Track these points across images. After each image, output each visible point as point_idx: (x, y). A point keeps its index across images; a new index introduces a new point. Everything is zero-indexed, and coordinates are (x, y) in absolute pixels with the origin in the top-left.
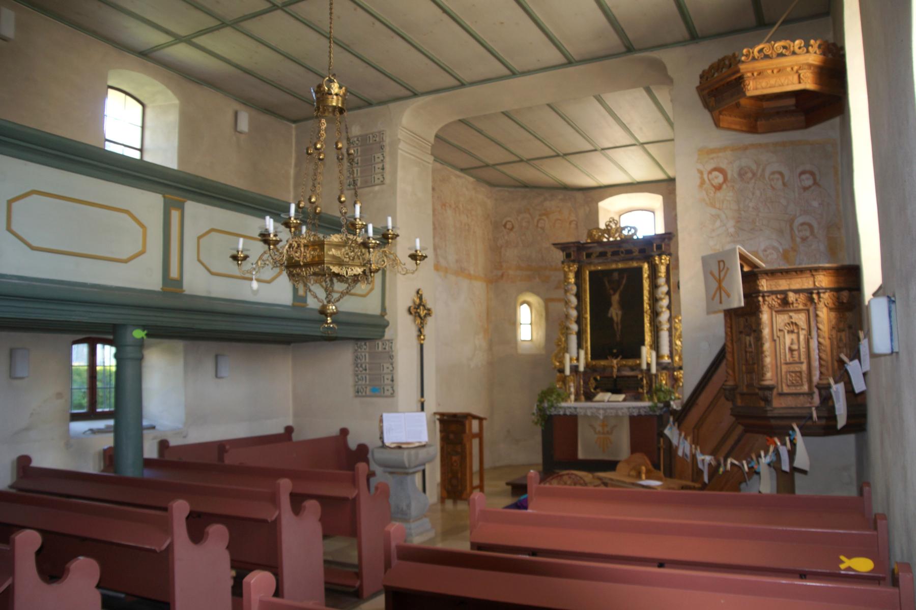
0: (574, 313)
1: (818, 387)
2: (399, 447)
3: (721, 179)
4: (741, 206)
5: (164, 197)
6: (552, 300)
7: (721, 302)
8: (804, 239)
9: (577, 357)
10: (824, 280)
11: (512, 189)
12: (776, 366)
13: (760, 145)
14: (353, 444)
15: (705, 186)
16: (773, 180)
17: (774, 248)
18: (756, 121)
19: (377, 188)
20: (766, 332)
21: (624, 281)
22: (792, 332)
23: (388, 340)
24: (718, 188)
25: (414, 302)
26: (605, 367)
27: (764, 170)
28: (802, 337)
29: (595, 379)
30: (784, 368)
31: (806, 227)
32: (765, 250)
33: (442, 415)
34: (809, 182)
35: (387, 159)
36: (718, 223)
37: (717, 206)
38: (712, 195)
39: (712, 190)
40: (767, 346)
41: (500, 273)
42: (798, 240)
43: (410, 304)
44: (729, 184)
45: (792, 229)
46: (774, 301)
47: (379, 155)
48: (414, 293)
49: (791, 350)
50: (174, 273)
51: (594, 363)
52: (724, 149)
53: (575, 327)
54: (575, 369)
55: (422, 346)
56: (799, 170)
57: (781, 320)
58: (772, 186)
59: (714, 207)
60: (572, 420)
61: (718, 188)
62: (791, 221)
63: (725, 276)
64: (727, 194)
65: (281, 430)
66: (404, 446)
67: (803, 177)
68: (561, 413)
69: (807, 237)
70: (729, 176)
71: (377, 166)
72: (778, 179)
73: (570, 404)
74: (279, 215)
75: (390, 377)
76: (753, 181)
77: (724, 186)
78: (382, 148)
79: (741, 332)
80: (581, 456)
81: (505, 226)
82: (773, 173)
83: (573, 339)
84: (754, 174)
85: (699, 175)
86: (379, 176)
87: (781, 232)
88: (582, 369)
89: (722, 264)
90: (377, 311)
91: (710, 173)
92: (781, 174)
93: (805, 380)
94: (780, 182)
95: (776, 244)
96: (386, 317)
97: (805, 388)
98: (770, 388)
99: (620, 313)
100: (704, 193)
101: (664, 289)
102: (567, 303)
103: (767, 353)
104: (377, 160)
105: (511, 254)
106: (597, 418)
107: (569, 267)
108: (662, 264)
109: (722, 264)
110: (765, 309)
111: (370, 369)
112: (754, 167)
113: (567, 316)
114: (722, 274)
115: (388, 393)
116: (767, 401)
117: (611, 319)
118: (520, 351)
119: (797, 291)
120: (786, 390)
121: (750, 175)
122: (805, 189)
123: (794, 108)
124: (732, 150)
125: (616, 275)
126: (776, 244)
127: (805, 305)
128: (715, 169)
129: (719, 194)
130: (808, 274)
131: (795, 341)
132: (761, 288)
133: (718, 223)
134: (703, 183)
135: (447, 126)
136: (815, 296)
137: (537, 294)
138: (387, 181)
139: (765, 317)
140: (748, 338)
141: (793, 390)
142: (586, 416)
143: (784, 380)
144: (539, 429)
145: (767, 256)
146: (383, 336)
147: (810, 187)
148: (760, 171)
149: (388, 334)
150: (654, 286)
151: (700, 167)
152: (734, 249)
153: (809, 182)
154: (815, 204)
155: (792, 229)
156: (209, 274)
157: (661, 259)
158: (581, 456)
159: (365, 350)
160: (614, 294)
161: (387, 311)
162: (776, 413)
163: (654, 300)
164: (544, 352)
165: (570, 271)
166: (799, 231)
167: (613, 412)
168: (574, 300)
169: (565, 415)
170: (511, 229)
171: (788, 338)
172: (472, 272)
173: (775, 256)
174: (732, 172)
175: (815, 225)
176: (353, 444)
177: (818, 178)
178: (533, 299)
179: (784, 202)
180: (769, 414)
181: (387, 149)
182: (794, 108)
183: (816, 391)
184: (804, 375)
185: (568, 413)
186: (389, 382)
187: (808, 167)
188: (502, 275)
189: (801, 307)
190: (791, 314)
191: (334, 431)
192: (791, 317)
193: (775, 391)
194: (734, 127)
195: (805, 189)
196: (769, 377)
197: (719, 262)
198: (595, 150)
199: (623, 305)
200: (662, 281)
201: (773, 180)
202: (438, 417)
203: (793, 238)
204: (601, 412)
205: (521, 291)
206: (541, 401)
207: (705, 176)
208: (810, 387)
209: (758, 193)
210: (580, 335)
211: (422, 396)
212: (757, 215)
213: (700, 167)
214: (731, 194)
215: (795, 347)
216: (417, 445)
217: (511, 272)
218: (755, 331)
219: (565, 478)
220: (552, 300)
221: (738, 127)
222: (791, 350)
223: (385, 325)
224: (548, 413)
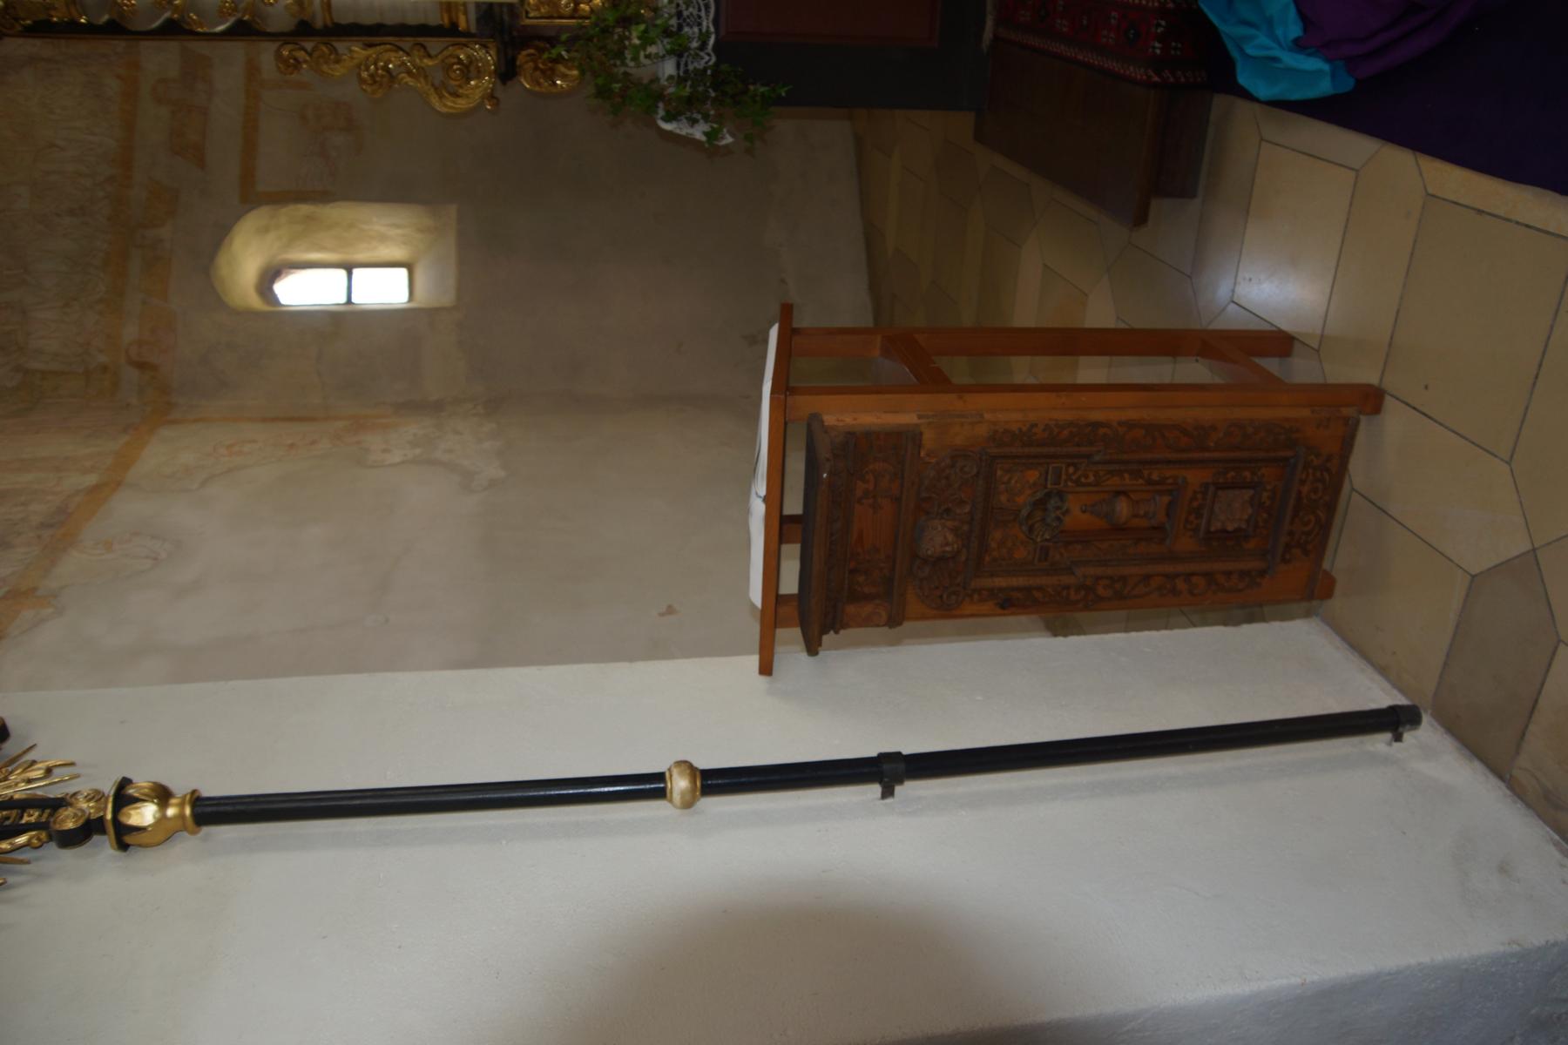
33: (776, 611)
118: (447, 299)
137: (220, 234)
164: (453, 210)
172: (92, 479)
178: (244, 258)
188: (142, 366)
202: (790, 641)
205: (211, 294)
211: (648, 787)
217: (130, 332)
224: (708, 59)
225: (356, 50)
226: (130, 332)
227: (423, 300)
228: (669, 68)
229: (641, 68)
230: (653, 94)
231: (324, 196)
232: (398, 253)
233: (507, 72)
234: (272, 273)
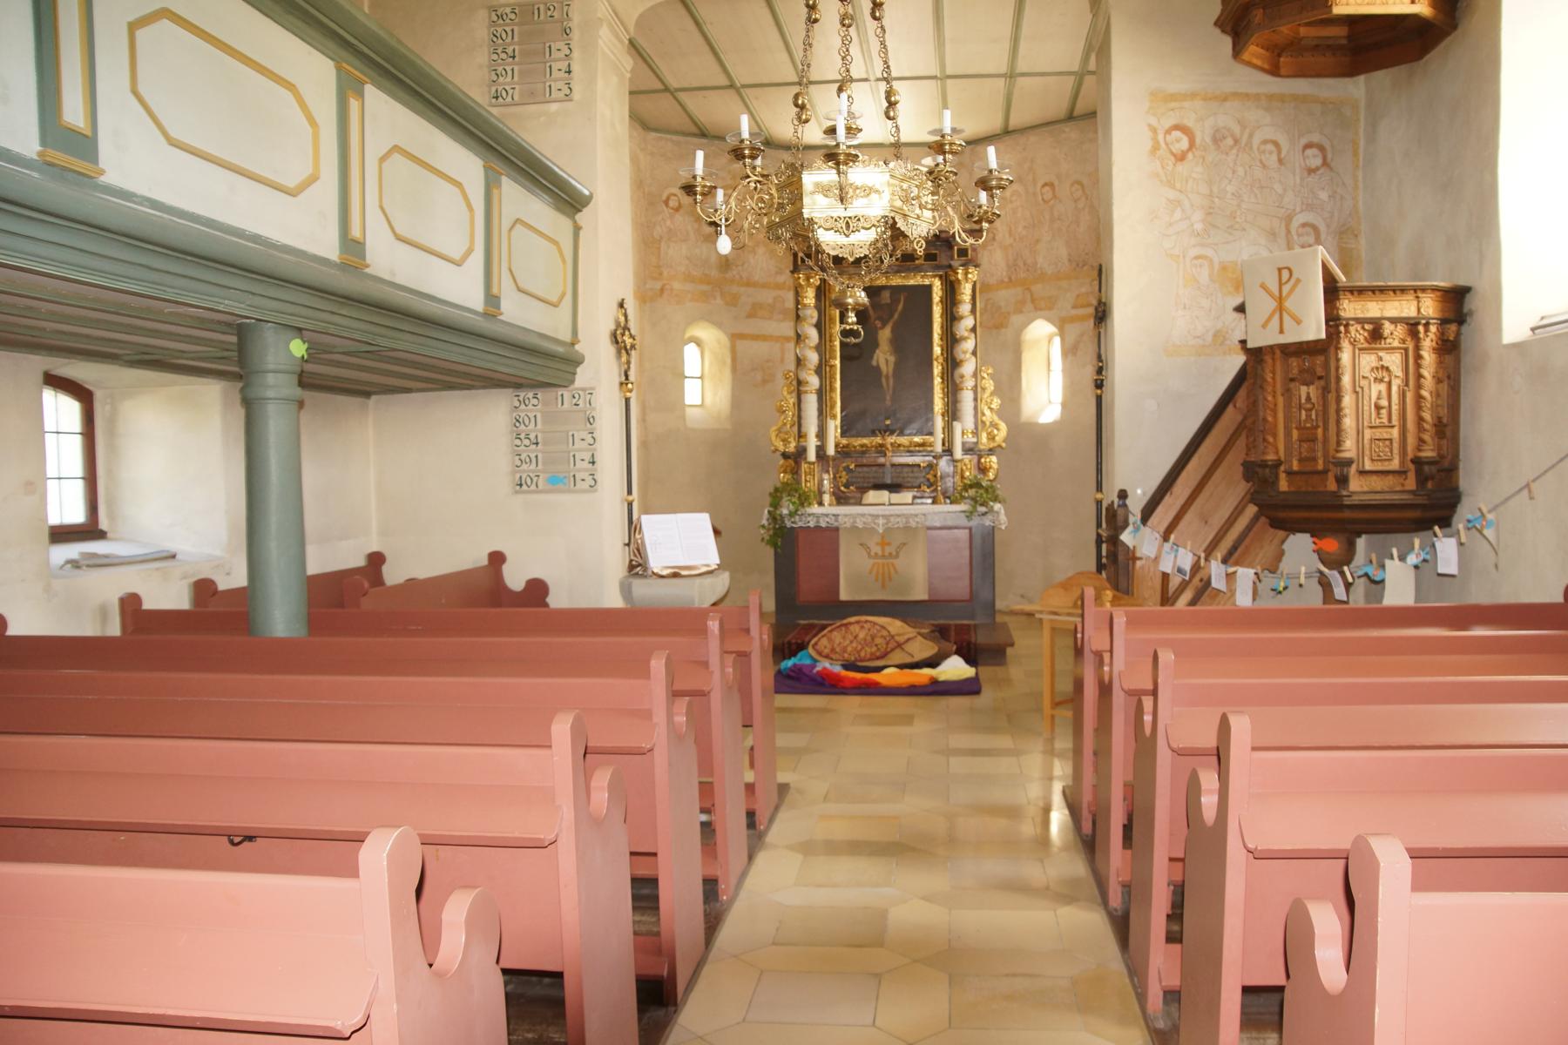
0: (813, 358)
1: (1412, 461)
2: (675, 575)
4: (1215, 190)
5: (339, 69)
6: (742, 336)
7: (1281, 331)
9: (824, 431)
10: (1429, 307)
11: (681, 138)
12: (1359, 432)
14: (515, 578)
15: (1159, 153)
18: (1279, 55)
19: (554, 107)
20: (1346, 380)
21: (900, 307)
22: (1381, 381)
23: (584, 390)
24: (1181, 157)
25: (618, 324)
26: (864, 451)
27: (1251, 136)
28: (1394, 389)
29: (847, 469)
30: (1368, 434)
31: (1309, 230)
35: (575, 54)
36: (1178, 215)
37: (1178, 185)
38: (1170, 168)
40: (1348, 401)
41: (658, 285)
43: (613, 327)
44: (1198, 153)
45: (1288, 232)
46: (1358, 333)
47: (561, 45)
48: (615, 306)
49: (1378, 408)
50: (356, 232)
51: (844, 441)
52: (1193, 96)
53: (814, 381)
54: (821, 450)
55: (627, 400)
56: (1304, 141)
57: (1368, 361)
59: (1173, 187)
60: (829, 535)
61: (1181, 157)
62: (1288, 219)
63: (1289, 294)
64: (1192, 169)
65: (359, 561)
66: (684, 573)
67: (1309, 152)
68: (812, 524)
70: (1198, 141)
71: (555, 66)
73: (825, 511)
74: (945, 106)
75: (587, 457)
77: (1190, 155)
78: (566, 32)
79: (1292, 380)
80: (844, 596)
81: (666, 203)
82: (1265, 142)
83: (811, 402)
84: (1236, 141)
86: (560, 85)
87: (1273, 234)
88: (831, 451)
89: (1285, 274)
90: (566, 336)
91: (1168, 132)
92: (1276, 144)
93: (1396, 451)
94: (1274, 157)
96: (577, 347)
97: (1395, 464)
98: (1349, 462)
99: (892, 359)
101: (968, 322)
102: (799, 338)
103: (1347, 411)
104: (555, 55)
105: (677, 254)
106: (872, 531)
107: (808, 279)
108: (966, 279)
109: (1285, 274)
110: (1345, 344)
111: (545, 444)
112: (1237, 130)
113: (799, 362)
114: (1286, 289)
115: (585, 485)
116: (1343, 481)
117: (878, 368)
118: (689, 424)
119: (1394, 321)
120: (1368, 466)
121: (1230, 141)
122: (1311, 171)
123: (1344, 42)
124: (1205, 99)
125: (886, 295)
127: (1404, 341)
128: (1176, 127)
129: (1180, 167)
130: (1411, 296)
131: (1384, 393)
132: (1342, 314)
133: (1178, 215)
134: (1156, 148)
135: (652, 8)
136: (1421, 328)
137: (719, 325)
138: (576, 95)
139: (1346, 356)
140: (1304, 389)
141: (1379, 467)
142: (854, 528)
143: (1367, 452)
144: (768, 555)
146: (573, 382)
147: (1317, 169)
149: (582, 377)
150: (951, 318)
151: (1153, 121)
152: (1316, 252)
154: (1324, 196)
155: (1288, 232)
156: (392, 238)
157: (966, 274)
158: (844, 596)
159: (535, 405)
160: (883, 327)
161: (580, 336)
162: (1356, 500)
163: (951, 340)
165: (809, 285)
167: (901, 522)
168: (813, 334)
169: (818, 528)
170: (677, 210)
171: (1377, 389)
174: (1203, 135)
175: (1322, 228)
176: (515, 578)
177: (1329, 156)
178: (709, 334)
179: (1278, 188)
180: (1347, 502)
181: (576, 35)
182: (1344, 42)
183: (1412, 467)
184: (1396, 445)
185: (823, 525)
186: (586, 465)
187: (1316, 138)
188: (662, 290)
189: (1396, 344)
190: (1381, 354)
191: (476, 557)
192: (1380, 359)
193: (1354, 467)
194: (1255, 61)
195: (1311, 171)
196: (1349, 448)
197: (1280, 270)
198: (866, 80)
199: (897, 344)
200: (965, 309)
204: (881, 521)
205: (691, 321)
206: (776, 505)
207: (1161, 137)
208: (1402, 462)
209: (1240, 171)
210: (821, 393)
212: (1239, 206)
213: (1153, 121)
214: (1199, 169)
215: (1384, 403)
216: (704, 569)
217: (677, 285)
218: (1320, 378)
219: (855, 629)
220: (742, 336)
221: (1259, 63)
222: (1378, 408)
223: (574, 361)
224: (789, 524)
225: (792, 400)
226: (677, 285)
227: (689, 411)
228: (785, 511)
229: (785, 501)
230: (776, 505)
231: (734, 369)
232: (708, 401)
233: (785, 456)
234: (699, 343)
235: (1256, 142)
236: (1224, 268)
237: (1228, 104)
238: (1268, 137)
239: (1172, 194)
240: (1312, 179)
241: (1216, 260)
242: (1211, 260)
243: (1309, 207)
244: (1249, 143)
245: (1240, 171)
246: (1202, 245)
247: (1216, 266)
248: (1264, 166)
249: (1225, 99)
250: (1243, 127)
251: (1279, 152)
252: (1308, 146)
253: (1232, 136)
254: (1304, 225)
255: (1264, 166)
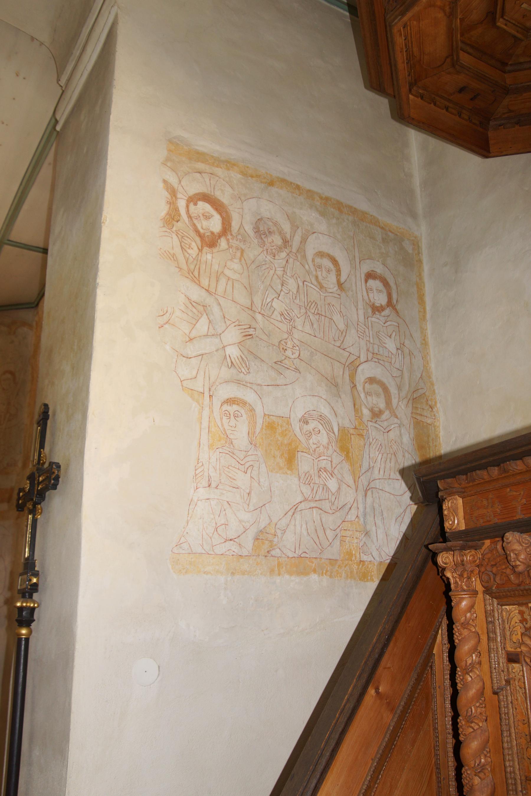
3: (215, 224)
4: (258, 301)
8: (376, 414)
13: (298, 187)
16: (320, 267)
17: (321, 418)
24: (210, 242)
27: (304, 241)
32: (305, 421)
34: (381, 299)
36: (203, 326)
37: (205, 282)
38: (194, 252)
39: (194, 245)
42: (366, 412)
52: (229, 164)
56: (366, 267)
58: (317, 277)
62: (353, 368)
67: (371, 282)
69: (381, 412)
70: (235, 225)
72: (329, 271)
76: (283, 255)
77: (223, 243)
84: (286, 242)
85: (166, 194)
87: (333, 385)
92: (334, 261)
94: (333, 278)
95: (326, 411)
100: (174, 237)
112: (287, 228)
122: (376, 309)
124: (244, 174)
126: (326, 411)
129: (208, 256)
133: (203, 326)
134: (172, 217)
145: (309, 435)
148: (297, 239)
151: (173, 180)
153: (381, 299)
154: (391, 345)
166: (368, 394)
173: (323, 438)
174: (242, 218)
175: (393, 390)
177: (394, 296)
195: (376, 309)
201: (320, 267)
203: (357, 409)
207: (182, 204)
209: (292, 284)
212: (290, 333)
214: (236, 265)
235: (310, 253)
236: (271, 427)
237: (274, 190)
238: (325, 249)
239: (196, 294)
240: (377, 320)
241: (259, 410)
242: (252, 410)
243: (375, 357)
244: (301, 250)
245: (292, 284)
246: (238, 382)
247: (260, 421)
248: (321, 287)
249: (271, 184)
250: (295, 227)
251: (339, 272)
252: (370, 276)
253: (281, 233)
254: (372, 380)
255: (321, 287)
